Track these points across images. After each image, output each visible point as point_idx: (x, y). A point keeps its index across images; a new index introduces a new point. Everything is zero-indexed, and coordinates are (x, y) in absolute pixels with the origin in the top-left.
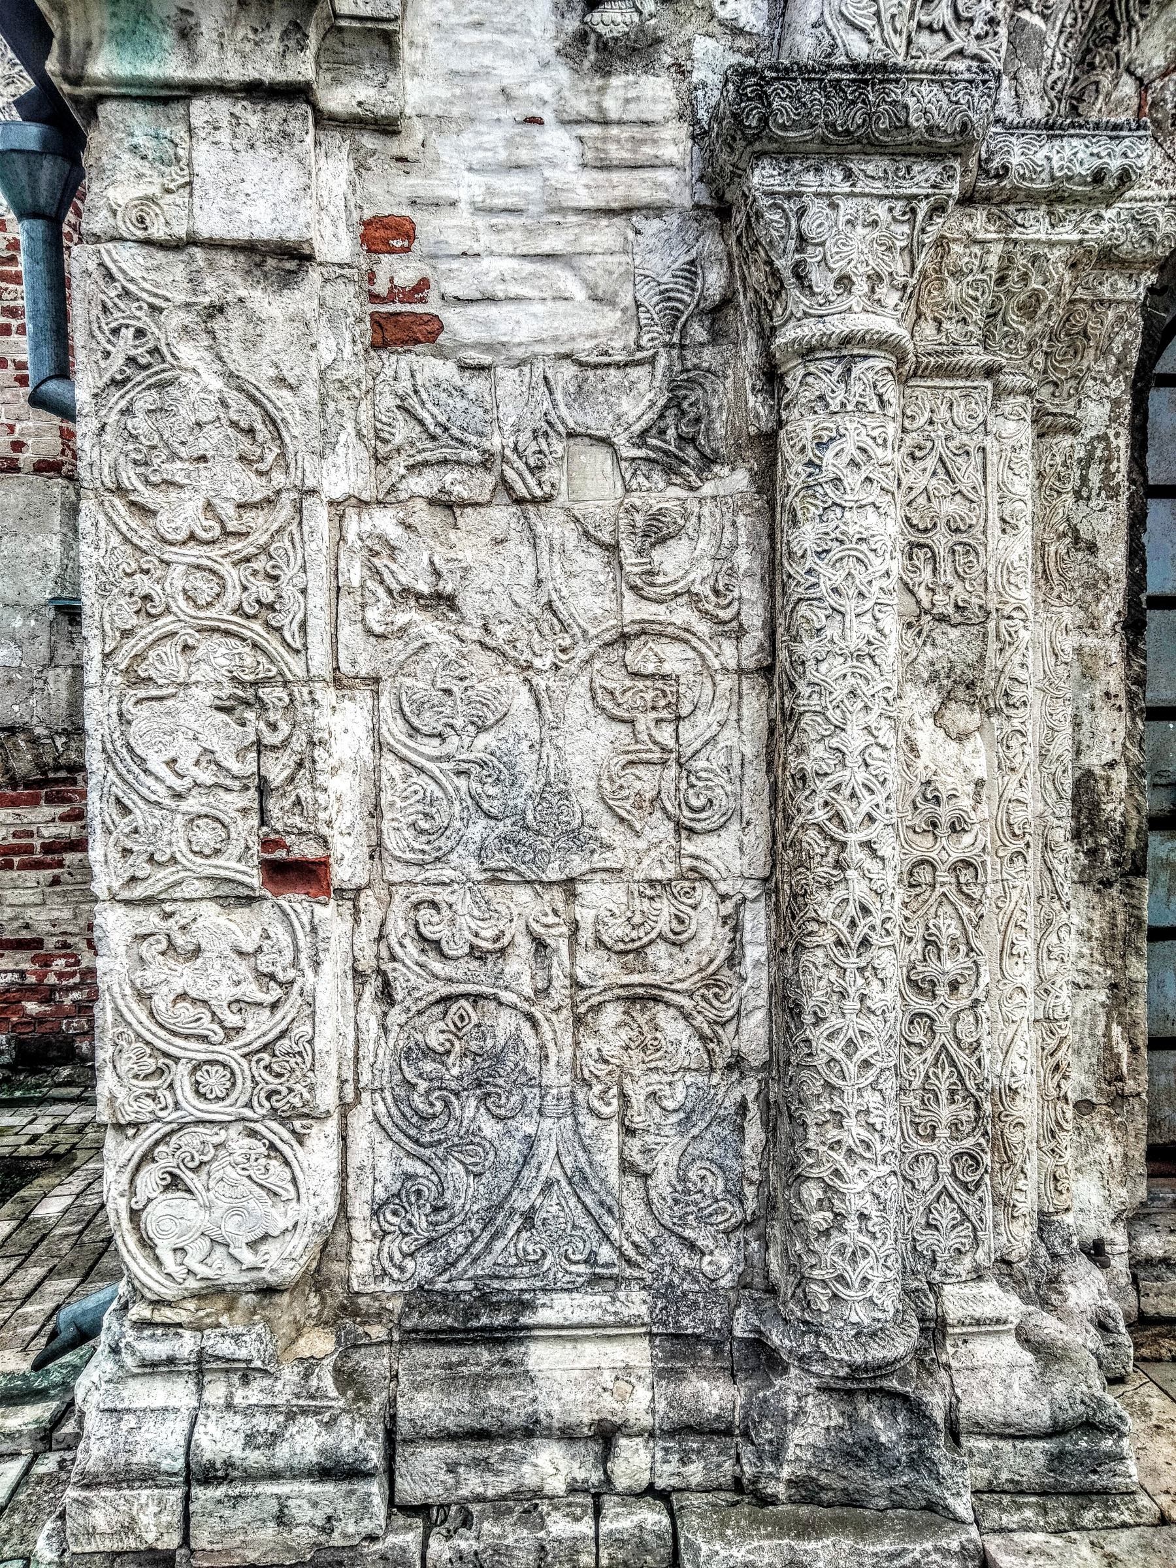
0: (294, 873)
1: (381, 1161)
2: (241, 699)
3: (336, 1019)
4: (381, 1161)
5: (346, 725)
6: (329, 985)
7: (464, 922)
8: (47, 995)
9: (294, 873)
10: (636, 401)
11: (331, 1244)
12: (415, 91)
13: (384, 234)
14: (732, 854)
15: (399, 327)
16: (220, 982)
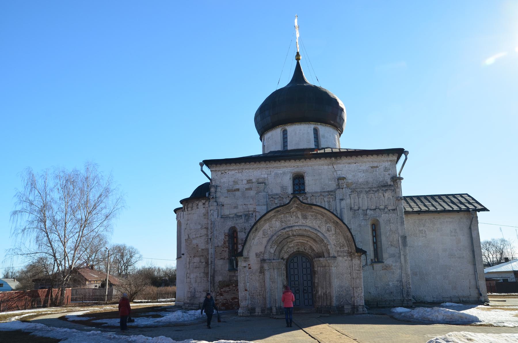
0: (246, 290)
1: (250, 302)
2: (244, 283)
3: (248, 296)
4: (250, 302)
5: (248, 284)
6: (247, 295)
7: (253, 292)
8: (228, 303)
9: (246, 290)
10: (259, 271)
11: (248, 305)
12: (250, 259)
13: (249, 265)
14: (263, 289)
15: (250, 268)
16: (243, 294)
